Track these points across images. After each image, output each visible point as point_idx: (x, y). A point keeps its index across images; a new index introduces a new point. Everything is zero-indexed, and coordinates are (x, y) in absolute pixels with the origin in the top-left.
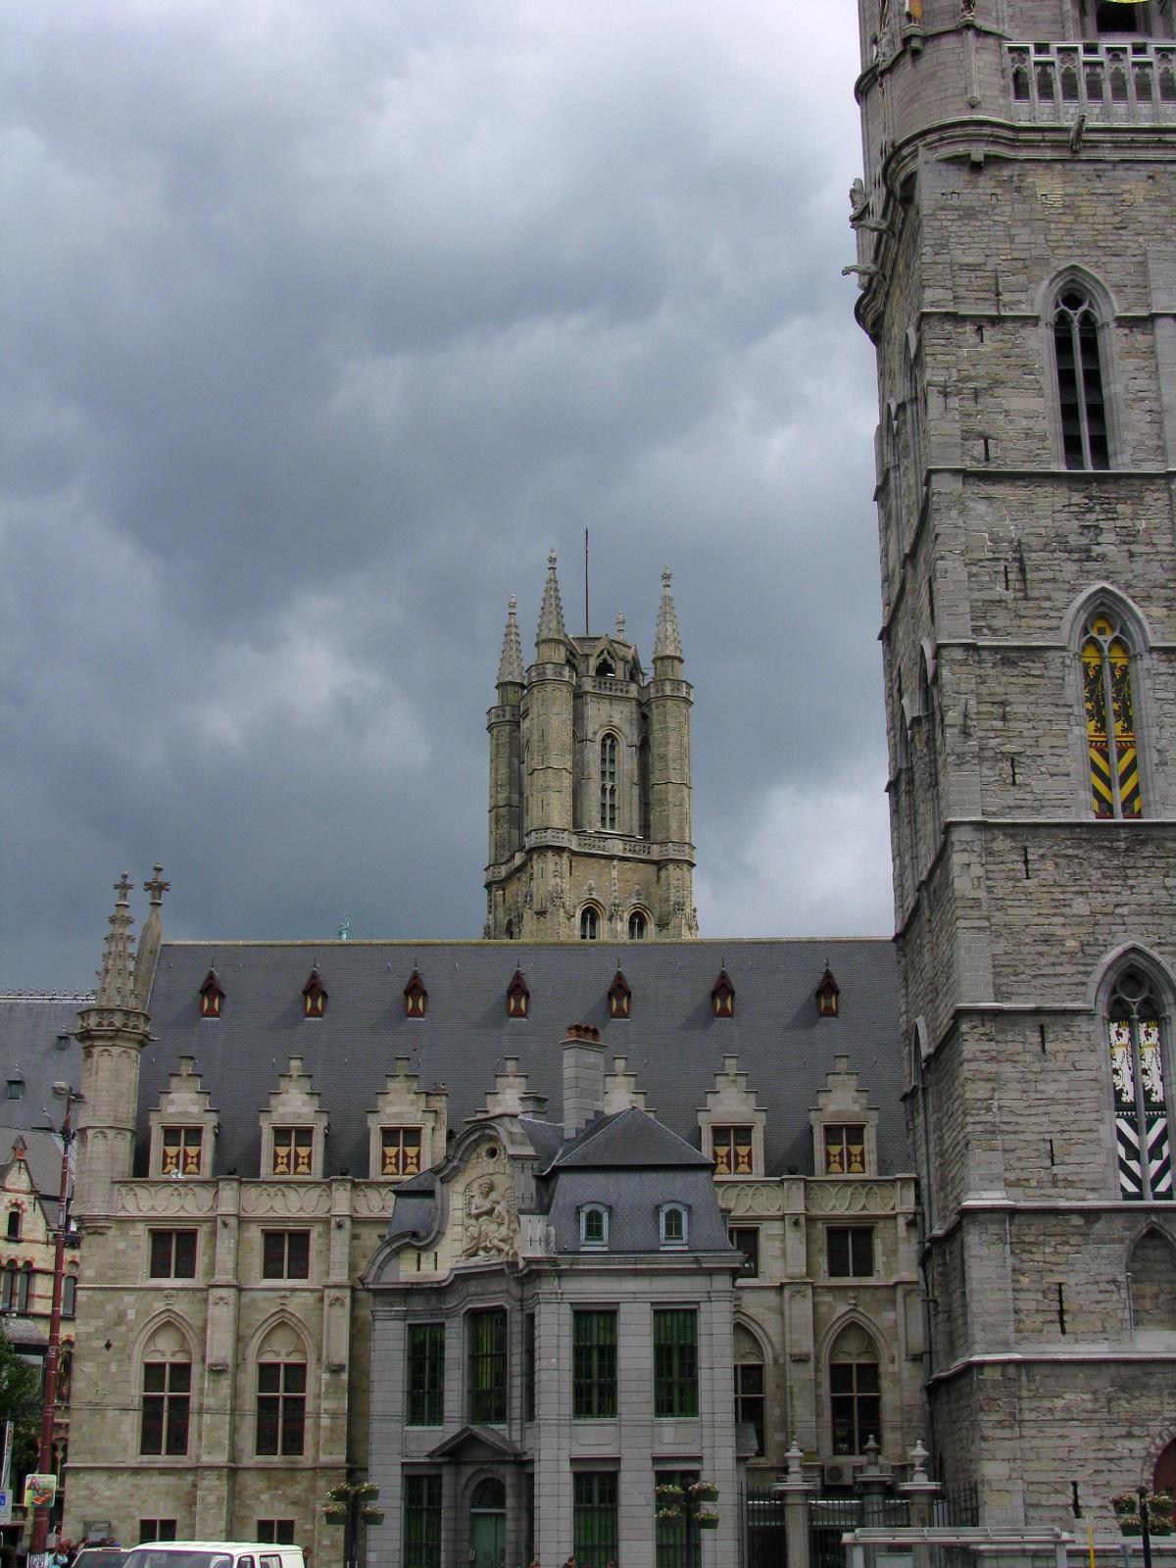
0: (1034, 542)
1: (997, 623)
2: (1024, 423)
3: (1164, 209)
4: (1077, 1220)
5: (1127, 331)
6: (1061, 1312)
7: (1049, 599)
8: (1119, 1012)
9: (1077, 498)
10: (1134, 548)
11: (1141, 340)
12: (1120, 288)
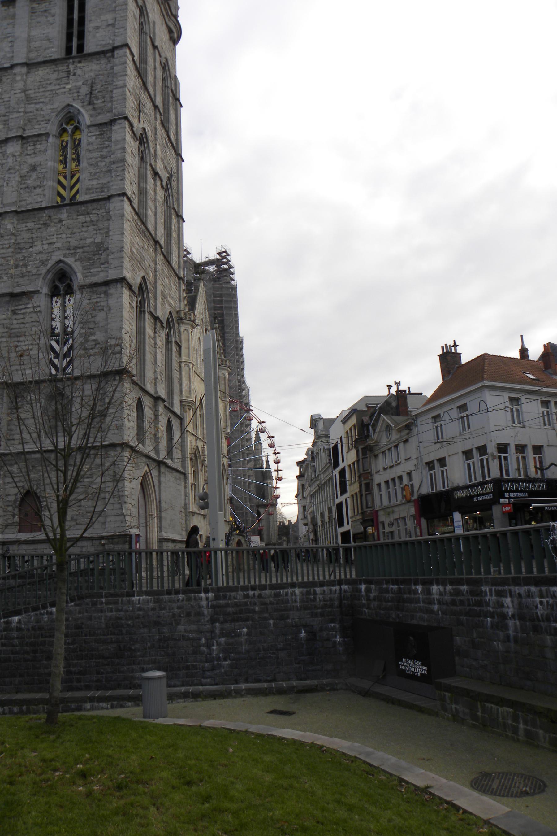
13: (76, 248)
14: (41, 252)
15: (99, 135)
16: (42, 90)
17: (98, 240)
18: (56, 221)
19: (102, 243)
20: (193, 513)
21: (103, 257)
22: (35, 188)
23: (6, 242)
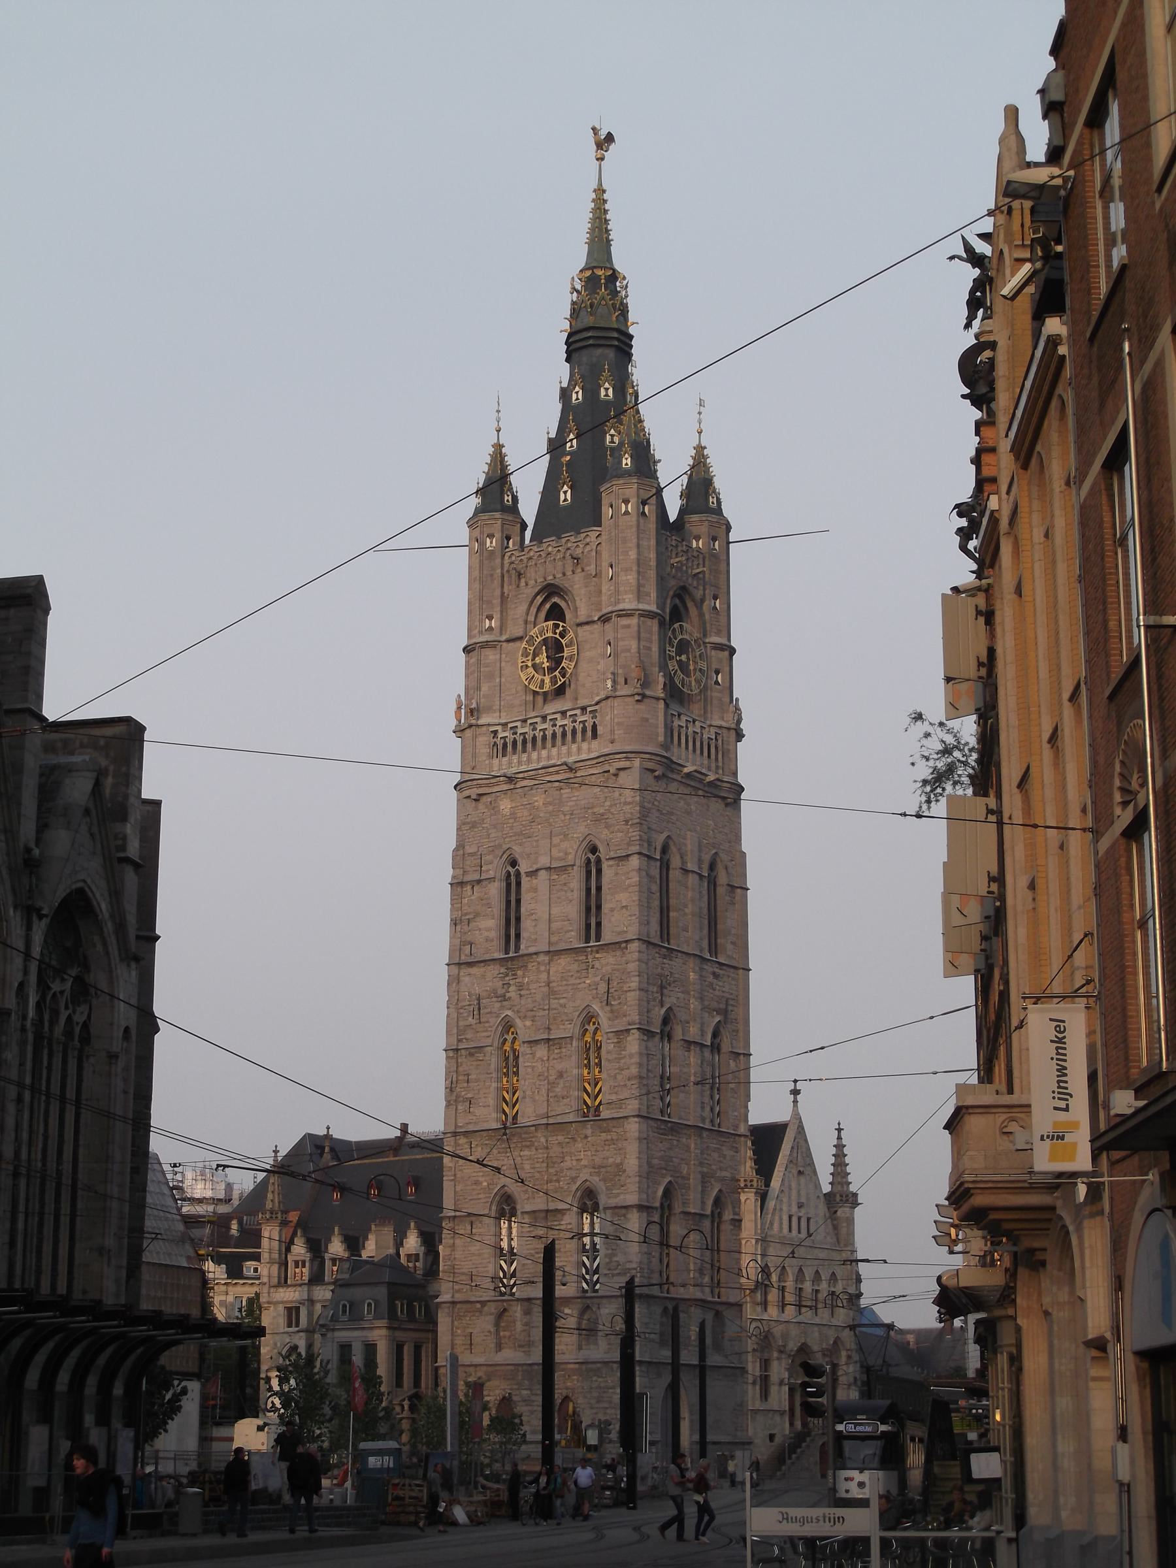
0: (484, 994)
1: (468, 1036)
2: (486, 934)
3: (550, 808)
4: (478, 1306)
5: (529, 878)
6: (471, 1344)
7: (488, 1022)
8: (501, 1214)
9: (503, 970)
10: (522, 992)
11: (535, 881)
12: (529, 855)
13: (600, 1167)
14: (570, 1169)
15: (618, 1042)
16: (564, 983)
17: (618, 1161)
18: (583, 1136)
19: (621, 1164)
20: (756, 1412)
21: (622, 1178)
22: (563, 1098)
23: (540, 1156)
